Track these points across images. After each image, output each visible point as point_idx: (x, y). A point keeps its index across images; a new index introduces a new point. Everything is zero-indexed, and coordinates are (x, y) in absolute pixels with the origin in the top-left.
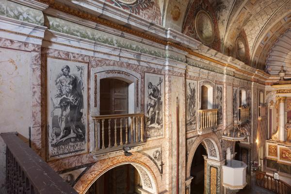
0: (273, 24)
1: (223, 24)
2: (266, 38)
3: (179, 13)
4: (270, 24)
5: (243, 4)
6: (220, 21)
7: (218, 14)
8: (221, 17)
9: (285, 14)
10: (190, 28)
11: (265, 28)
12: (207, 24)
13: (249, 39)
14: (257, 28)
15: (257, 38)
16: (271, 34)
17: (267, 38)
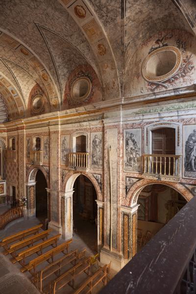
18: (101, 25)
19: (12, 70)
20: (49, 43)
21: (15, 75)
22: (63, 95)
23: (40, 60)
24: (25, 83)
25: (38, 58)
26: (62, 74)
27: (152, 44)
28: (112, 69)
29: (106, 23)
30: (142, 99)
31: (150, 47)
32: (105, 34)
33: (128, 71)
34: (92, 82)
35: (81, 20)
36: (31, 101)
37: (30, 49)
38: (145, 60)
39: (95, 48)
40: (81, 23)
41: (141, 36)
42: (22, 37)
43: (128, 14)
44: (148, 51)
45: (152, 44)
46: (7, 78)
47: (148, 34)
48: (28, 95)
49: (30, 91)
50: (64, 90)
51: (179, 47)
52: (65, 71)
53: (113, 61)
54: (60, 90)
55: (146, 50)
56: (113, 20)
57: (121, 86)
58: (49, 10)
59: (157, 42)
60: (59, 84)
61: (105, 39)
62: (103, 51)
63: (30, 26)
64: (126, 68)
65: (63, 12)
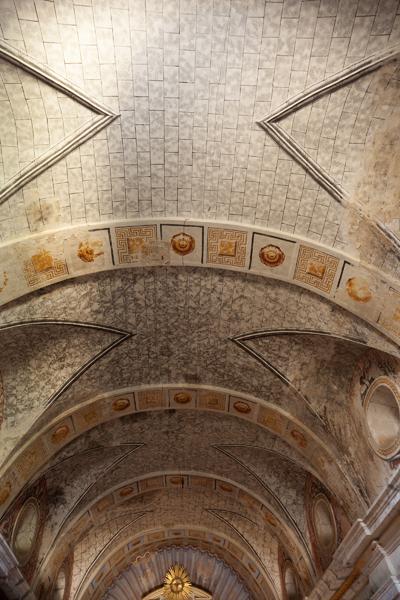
0: (114, 550)
1: (52, 531)
2: (100, 575)
3: (8, 495)
4: (109, 548)
5: (88, 507)
6: (50, 523)
7: (51, 510)
8: (54, 517)
9: (131, 538)
10: (6, 526)
11: (103, 555)
12: (30, 524)
13: (75, 570)
14: (93, 551)
15: (89, 572)
16: (108, 568)
17: (102, 575)
18: (274, 407)
19: (232, 523)
20: (244, 461)
21: (240, 530)
22: (310, 547)
23: (252, 493)
24: (261, 540)
25: (245, 489)
26: (290, 502)
27: (359, 389)
28: (330, 462)
29: (277, 401)
30: (388, 510)
31: (359, 396)
32: (287, 414)
33: (356, 453)
34: (329, 500)
35: (250, 415)
36: (283, 583)
37: (229, 481)
38: (364, 420)
39: (290, 440)
40: (253, 417)
41: (335, 388)
42: (211, 469)
43: (290, 377)
44: (360, 402)
45: (359, 389)
46: (233, 541)
47: (343, 379)
48: (276, 567)
49: (276, 557)
50: (308, 535)
51: (386, 374)
52: (292, 493)
53: (322, 449)
54: (301, 538)
55: (357, 402)
56: (281, 393)
57: (361, 491)
58: (216, 424)
59: (362, 383)
60: (295, 525)
61: (290, 422)
62: (303, 440)
63: (210, 452)
64: (351, 450)
65: (228, 418)
